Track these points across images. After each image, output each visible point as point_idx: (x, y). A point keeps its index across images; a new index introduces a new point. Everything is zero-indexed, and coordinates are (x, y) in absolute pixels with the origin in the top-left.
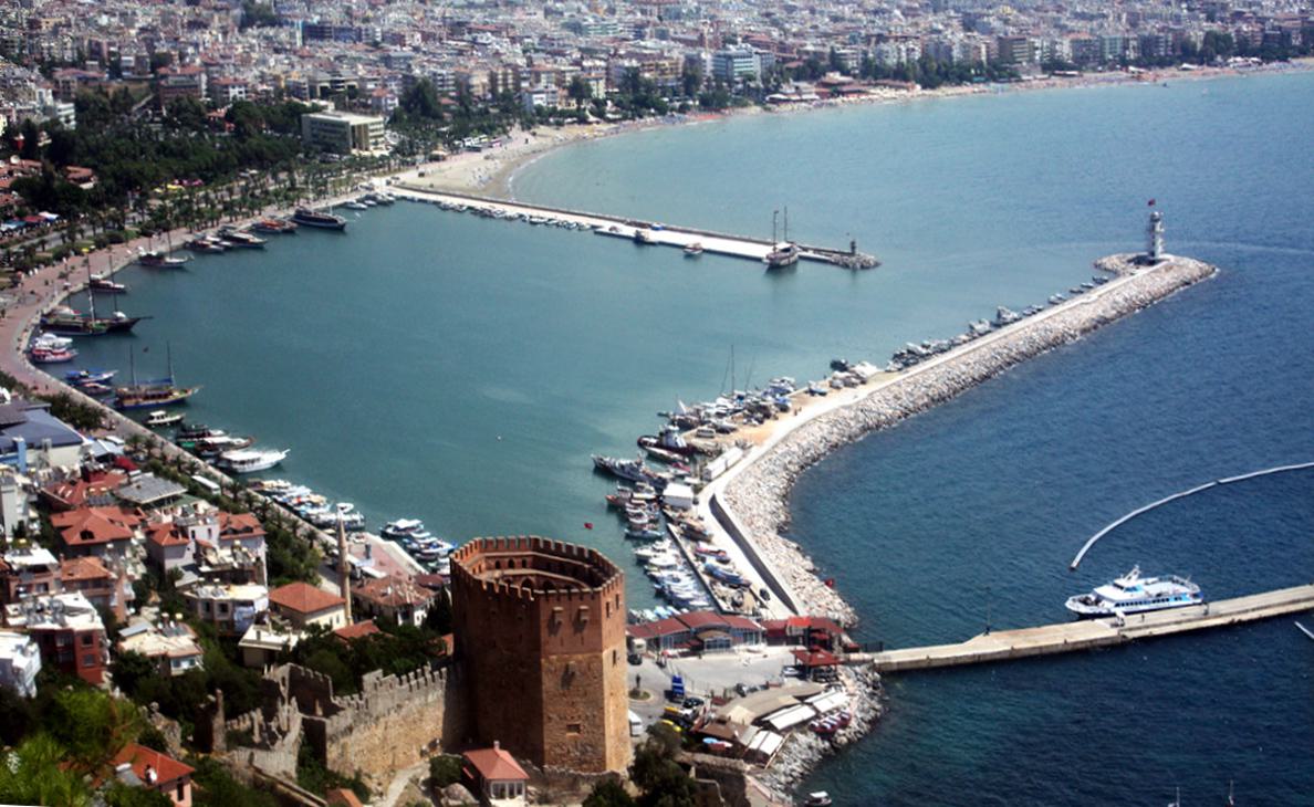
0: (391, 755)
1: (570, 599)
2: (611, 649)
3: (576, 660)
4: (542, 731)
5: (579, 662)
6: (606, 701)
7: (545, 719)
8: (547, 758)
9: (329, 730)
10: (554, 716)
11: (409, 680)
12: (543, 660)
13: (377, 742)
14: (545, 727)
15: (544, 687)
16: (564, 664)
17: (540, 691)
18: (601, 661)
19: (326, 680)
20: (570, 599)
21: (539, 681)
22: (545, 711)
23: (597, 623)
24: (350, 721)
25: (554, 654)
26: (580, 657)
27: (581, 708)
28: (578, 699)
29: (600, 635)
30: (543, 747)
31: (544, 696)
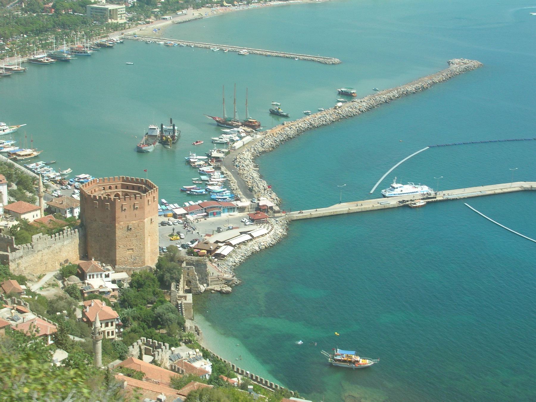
0: (45, 266)
1: (130, 200)
2: (150, 218)
3: (133, 223)
5: (133, 224)
6: (146, 238)
7: (117, 247)
8: (117, 263)
9: (10, 258)
10: (121, 246)
11: (55, 236)
12: (117, 225)
13: (38, 261)
14: (117, 250)
15: (116, 235)
16: (127, 225)
17: (115, 237)
18: (144, 223)
19: (12, 238)
20: (130, 200)
21: (115, 233)
22: (117, 244)
24: (21, 254)
25: (122, 222)
26: (134, 222)
27: (134, 242)
28: (133, 238)
29: (144, 213)
30: (116, 259)
31: (117, 239)
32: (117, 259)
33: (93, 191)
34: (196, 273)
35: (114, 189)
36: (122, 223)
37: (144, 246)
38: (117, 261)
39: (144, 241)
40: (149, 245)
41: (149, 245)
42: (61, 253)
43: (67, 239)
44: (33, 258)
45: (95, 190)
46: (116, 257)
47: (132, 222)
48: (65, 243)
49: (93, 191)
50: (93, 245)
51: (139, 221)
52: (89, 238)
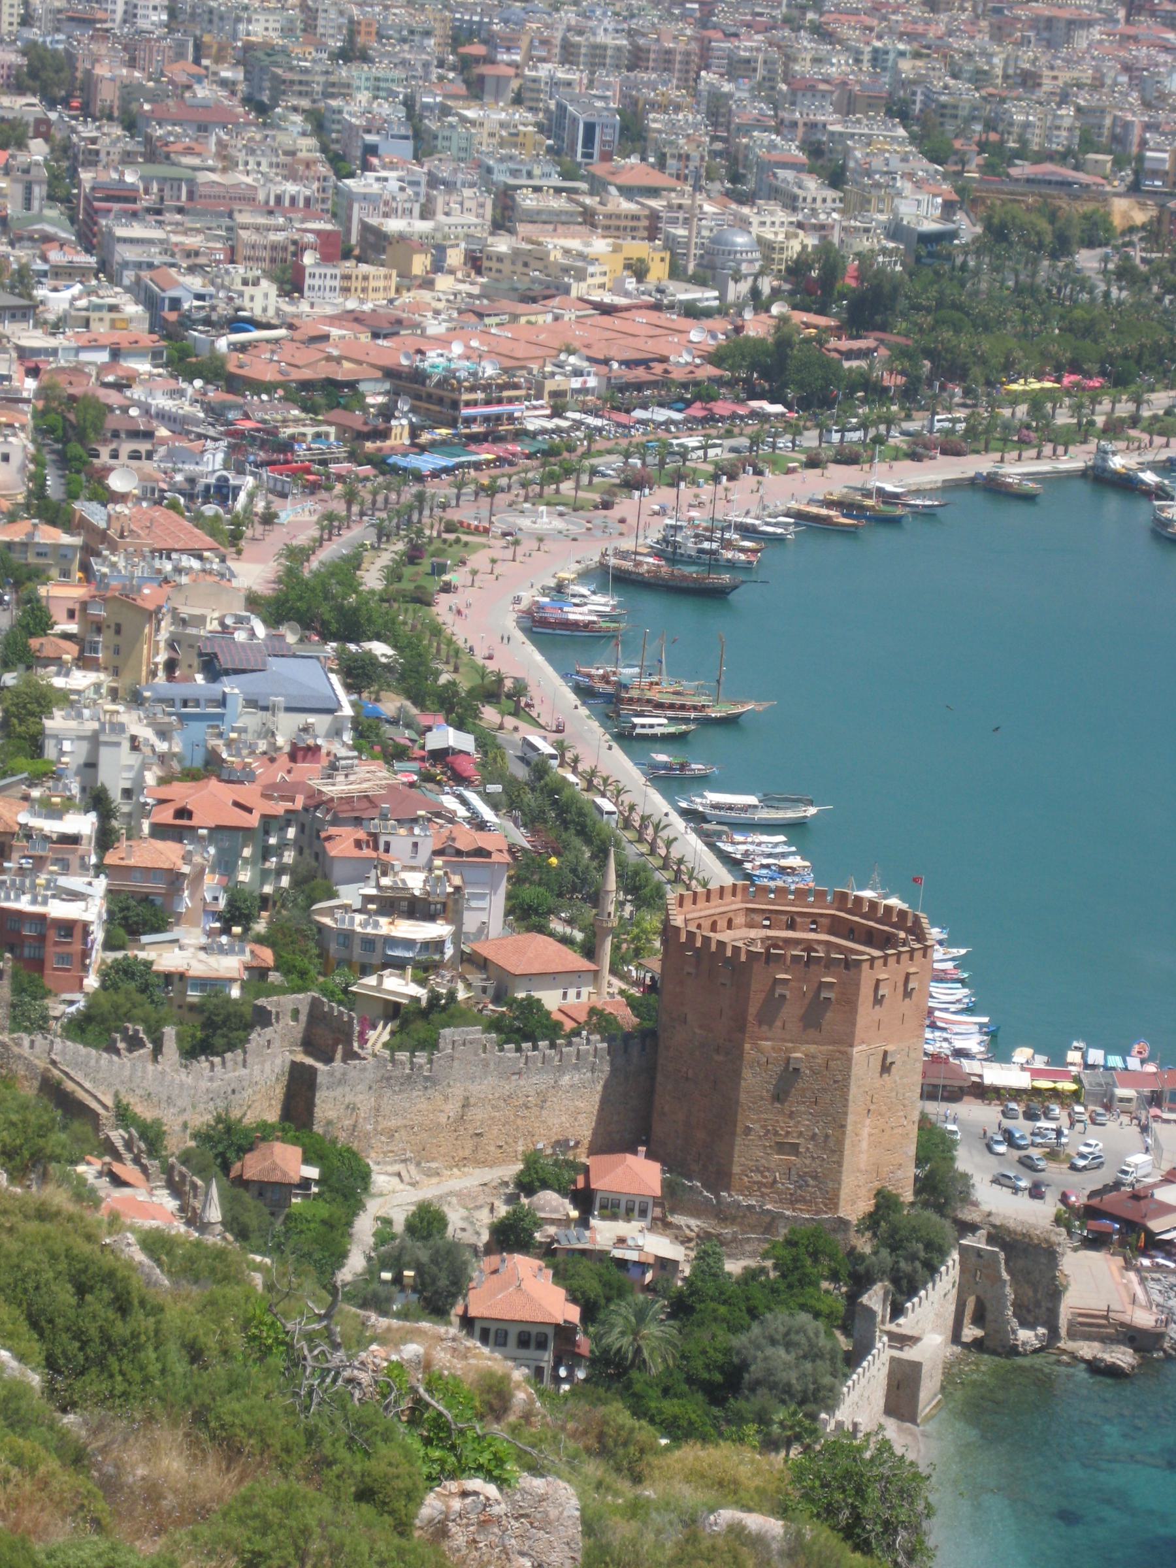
4: (732, 1146)
12: (747, 1046)
13: (443, 1120)
14: (739, 1140)
15: (743, 1083)
19: (351, 1018)
21: (737, 1074)
22: (739, 1117)
23: (849, 1004)
25: (767, 1039)
26: (813, 1048)
28: (802, 1108)
31: (743, 1097)
32: (736, 1169)
33: (723, 924)
34: (1005, 1276)
35: (804, 931)
37: (840, 1143)
38: (735, 1181)
39: (843, 1126)
40: (864, 1145)
41: (864, 1145)
42: (544, 1113)
43: (576, 1067)
44: (423, 1105)
45: (730, 921)
46: (731, 1162)
47: (804, 1048)
48: (566, 1080)
49: (723, 924)
50: (666, 1109)
52: (660, 1078)
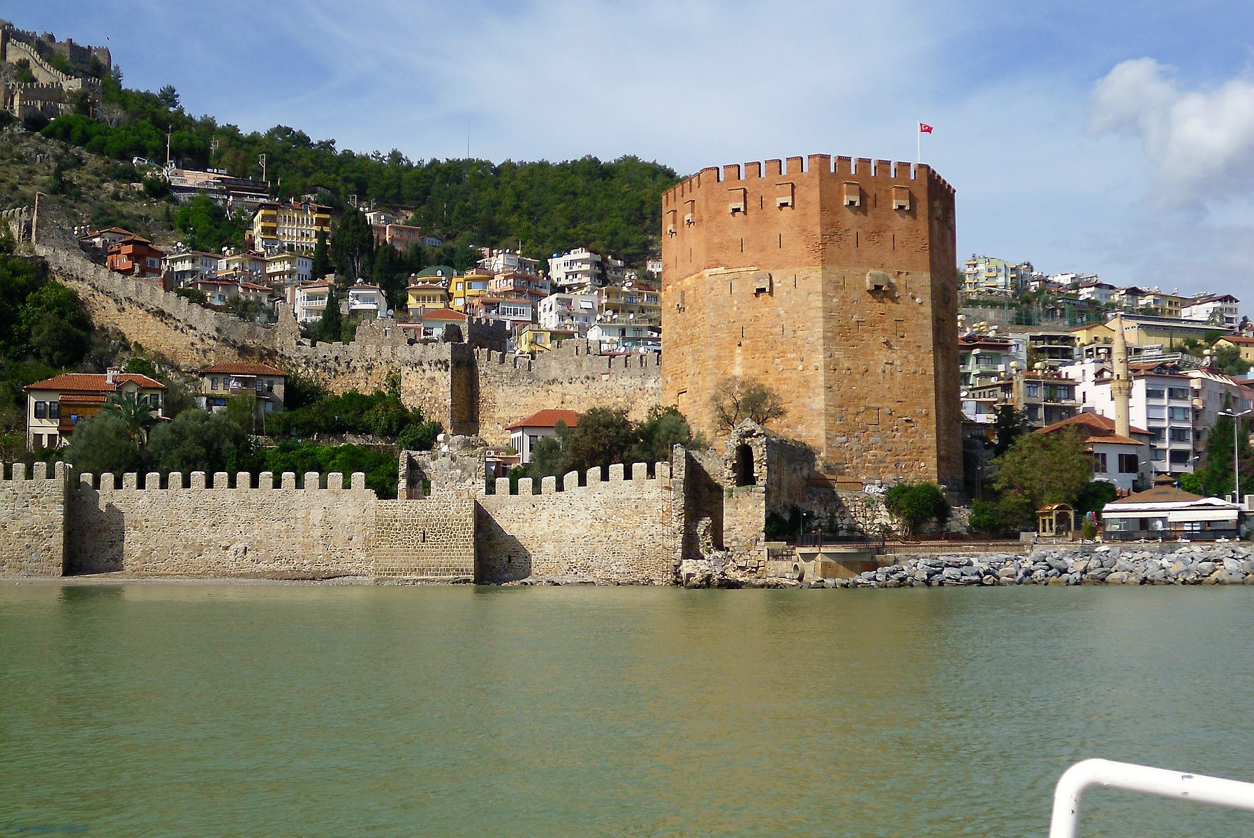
36: (671, 287)
44: (530, 400)
51: (696, 275)
